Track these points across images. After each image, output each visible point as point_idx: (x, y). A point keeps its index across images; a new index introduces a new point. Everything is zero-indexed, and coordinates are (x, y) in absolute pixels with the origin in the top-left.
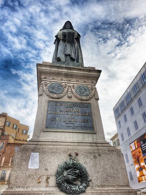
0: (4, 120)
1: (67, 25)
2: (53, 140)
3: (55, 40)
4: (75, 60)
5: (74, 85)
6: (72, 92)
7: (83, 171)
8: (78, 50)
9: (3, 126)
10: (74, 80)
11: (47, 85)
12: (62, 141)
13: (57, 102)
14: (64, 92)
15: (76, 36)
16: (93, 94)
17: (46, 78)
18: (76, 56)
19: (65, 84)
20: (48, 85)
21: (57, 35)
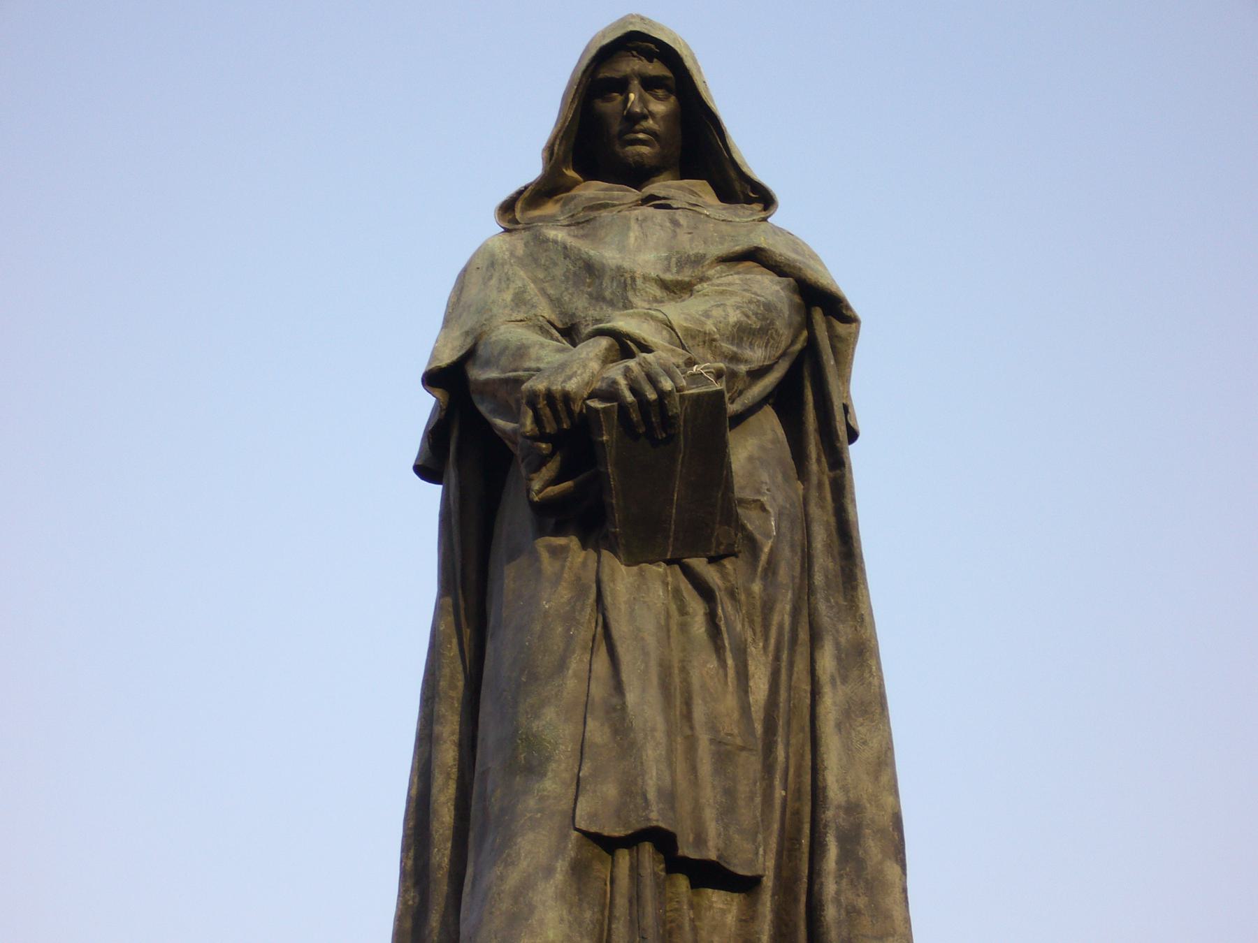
1: (610, 107)
3: (437, 436)
4: (746, 885)
15: (757, 374)
21: (470, 356)
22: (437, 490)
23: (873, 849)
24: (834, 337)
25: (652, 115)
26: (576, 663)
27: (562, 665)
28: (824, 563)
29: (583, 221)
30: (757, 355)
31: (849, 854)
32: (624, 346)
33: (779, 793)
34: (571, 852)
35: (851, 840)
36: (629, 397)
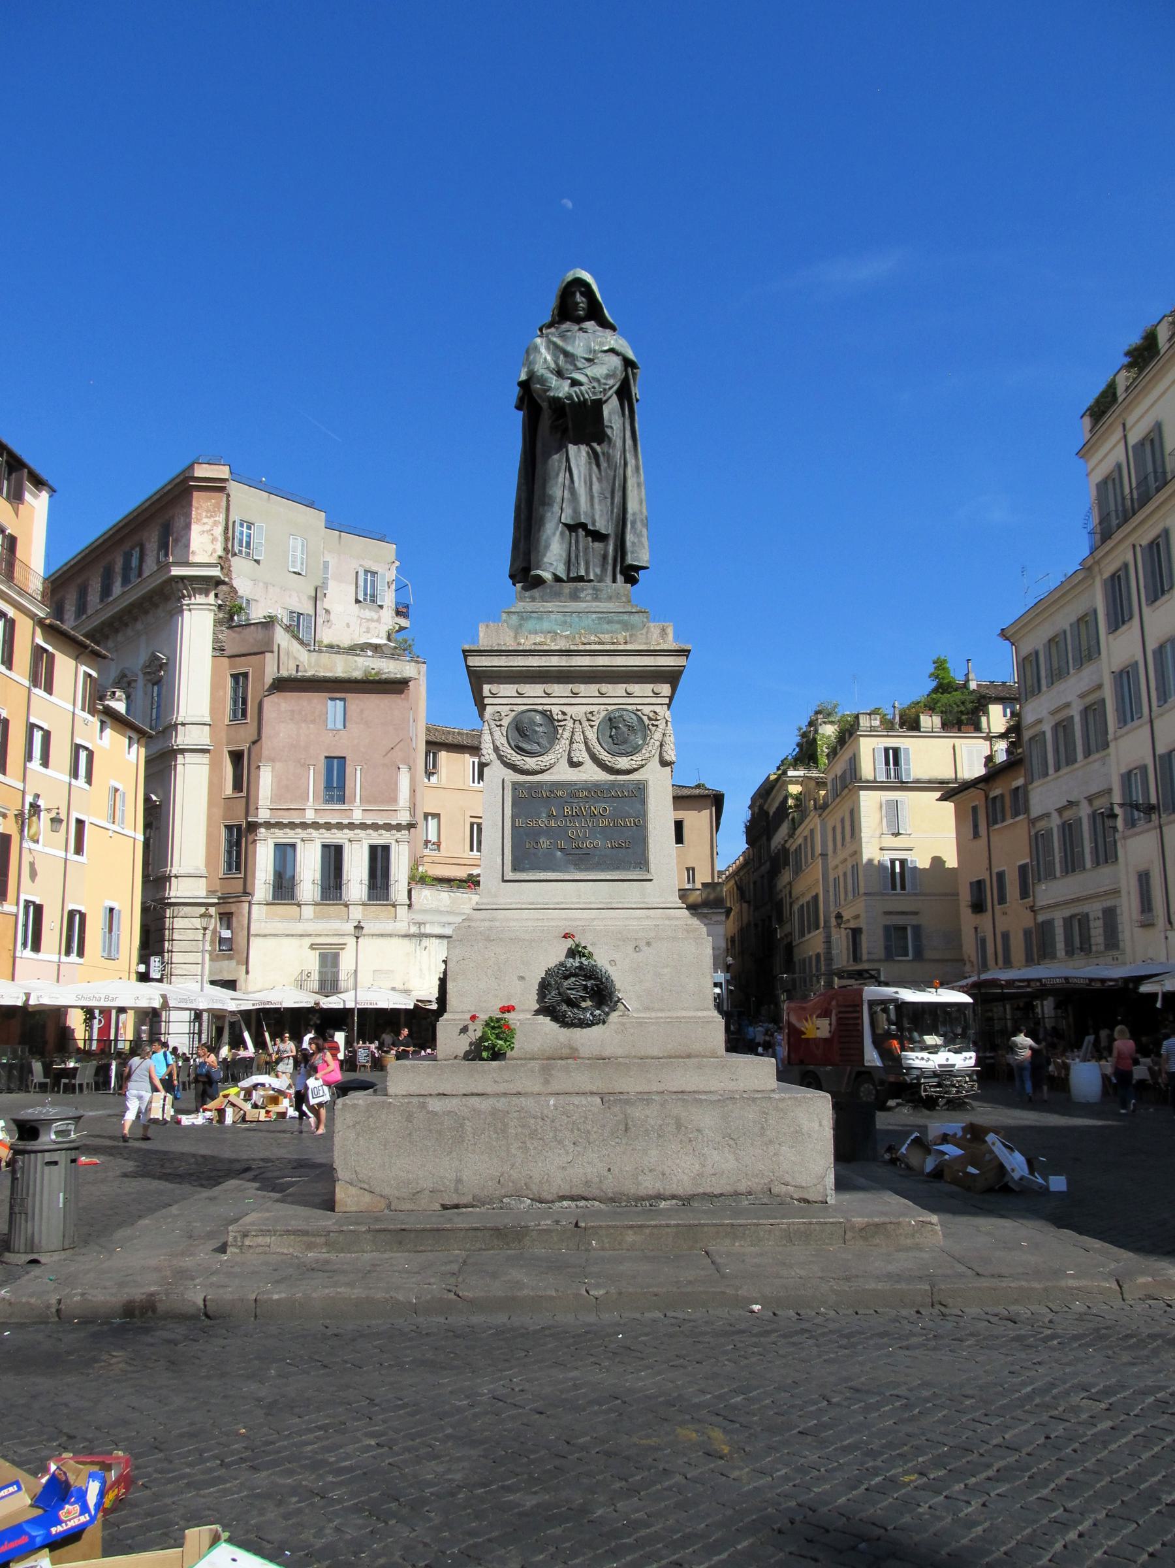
0: (221, 518)
2: (532, 903)
5: (591, 713)
6: (586, 743)
7: (601, 981)
8: (626, 464)
9: (214, 560)
10: (593, 689)
11: (502, 723)
12: (557, 906)
13: (540, 784)
14: (558, 747)
16: (658, 743)
17: (494, 696)
18: (612, 512)
19: (564, 713)
20: (505, 722)
22: (520, 414)
23: (639, 525)
24: (634, 374)
25: (582, 302)
26: (561, 475)
27: (558, 475)
28: (629, 442)
29: (562, 336)
30: (611, 382)
31: (633, 527)
32: (575, 383)
33: (615, 510)
34: (560, 529)
35: (633, 523)
36: (576, 399)
